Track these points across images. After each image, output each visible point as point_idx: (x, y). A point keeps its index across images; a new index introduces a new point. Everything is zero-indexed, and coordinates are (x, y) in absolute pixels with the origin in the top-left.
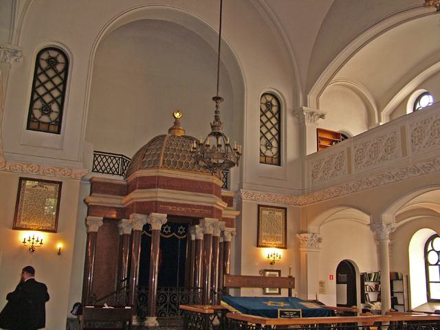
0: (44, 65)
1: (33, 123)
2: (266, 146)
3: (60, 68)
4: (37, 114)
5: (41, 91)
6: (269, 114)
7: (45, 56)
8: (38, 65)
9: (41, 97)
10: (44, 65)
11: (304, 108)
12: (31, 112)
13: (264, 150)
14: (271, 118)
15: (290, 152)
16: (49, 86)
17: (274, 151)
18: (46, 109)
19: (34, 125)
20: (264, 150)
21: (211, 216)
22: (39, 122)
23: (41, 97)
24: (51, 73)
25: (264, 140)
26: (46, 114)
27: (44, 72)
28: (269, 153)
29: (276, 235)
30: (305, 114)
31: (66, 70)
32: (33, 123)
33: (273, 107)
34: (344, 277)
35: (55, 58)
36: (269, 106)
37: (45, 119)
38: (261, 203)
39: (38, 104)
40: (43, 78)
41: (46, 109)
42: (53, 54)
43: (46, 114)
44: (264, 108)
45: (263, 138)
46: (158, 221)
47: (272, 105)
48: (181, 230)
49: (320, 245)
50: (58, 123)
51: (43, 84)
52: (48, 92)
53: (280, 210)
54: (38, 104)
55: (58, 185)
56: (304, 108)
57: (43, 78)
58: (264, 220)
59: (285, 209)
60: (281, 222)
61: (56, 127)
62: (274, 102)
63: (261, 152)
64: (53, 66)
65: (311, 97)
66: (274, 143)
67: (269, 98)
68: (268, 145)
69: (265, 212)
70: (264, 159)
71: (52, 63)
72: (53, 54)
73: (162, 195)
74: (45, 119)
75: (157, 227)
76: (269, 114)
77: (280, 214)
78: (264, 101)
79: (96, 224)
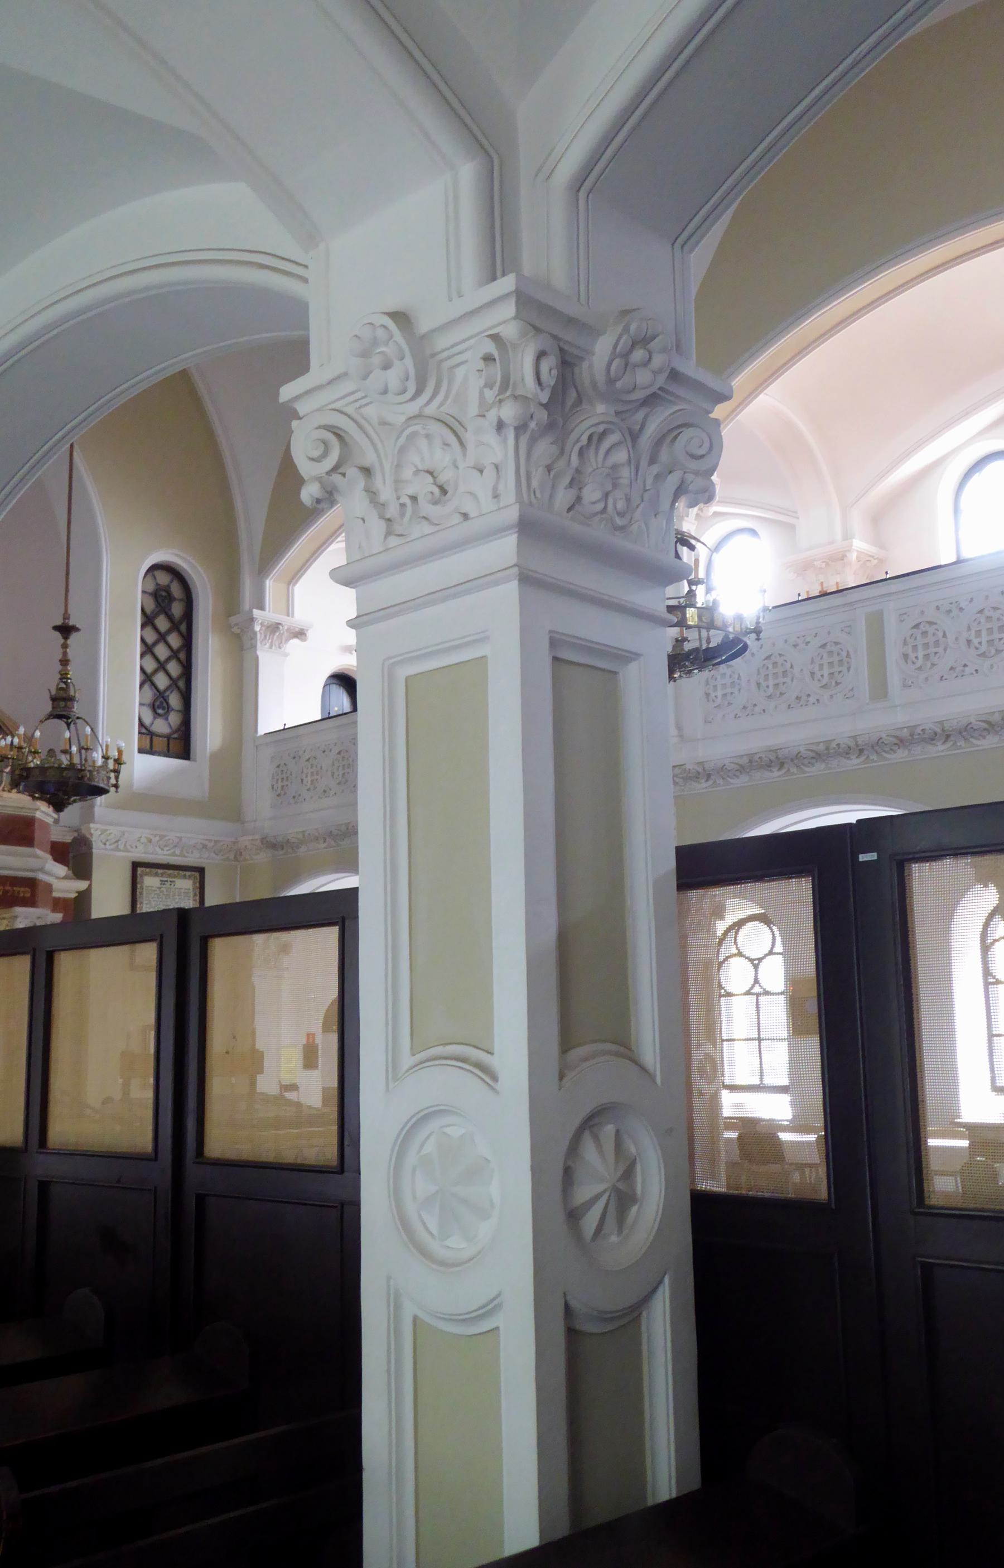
2: (154, 707)
11: (256, 612)
15: (210, 730)
17: (175, 719)
25: (149, 694)
28: (161, 727)
30: (257, 628)
33: (170, 608)
44: (151, 606)
45: (146, 687)
47: (171, 598)
53: (188, 873)
56: (256, 612)
59: (201, 871)
62: (176, 590)
63: (141, 724)
65: (270, 585)
66: (174, 700)
67: (163, 578)
68: (158, 705)
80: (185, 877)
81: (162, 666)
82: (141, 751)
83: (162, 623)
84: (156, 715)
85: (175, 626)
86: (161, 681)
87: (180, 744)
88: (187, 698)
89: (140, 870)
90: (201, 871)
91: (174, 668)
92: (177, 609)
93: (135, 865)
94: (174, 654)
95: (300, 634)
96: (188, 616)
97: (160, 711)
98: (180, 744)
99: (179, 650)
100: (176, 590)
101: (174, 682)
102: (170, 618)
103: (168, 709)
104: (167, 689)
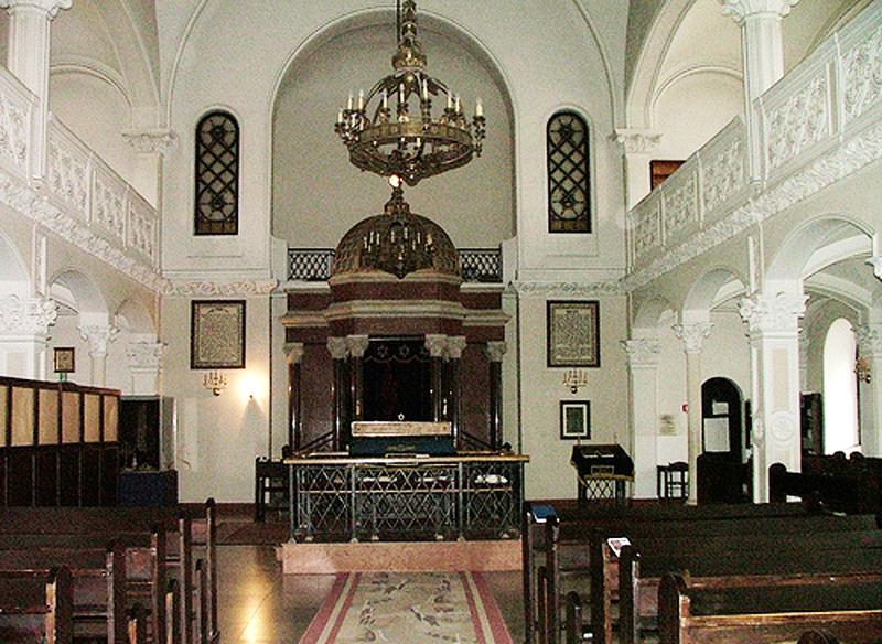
0: (208, 139)
1: (202, 226)
2: (562, 202)
3: (229, 139)
4: (206, 210)
5: (208, 177)
6: (566, 149)
7: (207, 127)
8: (199, 140)
9: (208, 187)
10: (208, 139)
13: (558, 208)
14: (571, 153)
16: (218, 168)
17: (579, 208)
18: (218, 202)
19: (205, 228)
20: (558, 208)
22: (211, 222)
24: (218, 150)
26: (215, 211)
27: (209, 150)
28: (569, 214)
29: (581, 346)
32: (202, 226)
34: (720, 407)
35: (221, 127)
36: (566, 133)
37: (218, 216)
39: (207, 197)
40: (208, 159)
43: (215, 211)
44: (556, 138)
47: (572, 132)
48: (405, 351)
50: (234, 218)
51: (209, 168)
54: (207, 197)
55: (241, 306)
61: (229, 226)
62: (576, 125)
64: (217, 139)
66: (578, 196)
68: (567, 200)
70: (557, 224)
71: (218, 133)
72: (218, 121)
74: (218, 216)
75: (358, 352)
76: (566, 149)
77: (585, 312)
78: (556, 126)
80: (584, 308)
81: (567, 176)
84: (565, 208)
85: (576, 149)
86: (568, 185)
89: (552, 305)
90: (596, 303)
92: (577, 138)
97: (568, 204)
98: (583, 224)
99: (581, 163)
100: (576, 125)
101: (577, 185)
102: (572, 144)
103: (573, 202)
104: (572, 190)
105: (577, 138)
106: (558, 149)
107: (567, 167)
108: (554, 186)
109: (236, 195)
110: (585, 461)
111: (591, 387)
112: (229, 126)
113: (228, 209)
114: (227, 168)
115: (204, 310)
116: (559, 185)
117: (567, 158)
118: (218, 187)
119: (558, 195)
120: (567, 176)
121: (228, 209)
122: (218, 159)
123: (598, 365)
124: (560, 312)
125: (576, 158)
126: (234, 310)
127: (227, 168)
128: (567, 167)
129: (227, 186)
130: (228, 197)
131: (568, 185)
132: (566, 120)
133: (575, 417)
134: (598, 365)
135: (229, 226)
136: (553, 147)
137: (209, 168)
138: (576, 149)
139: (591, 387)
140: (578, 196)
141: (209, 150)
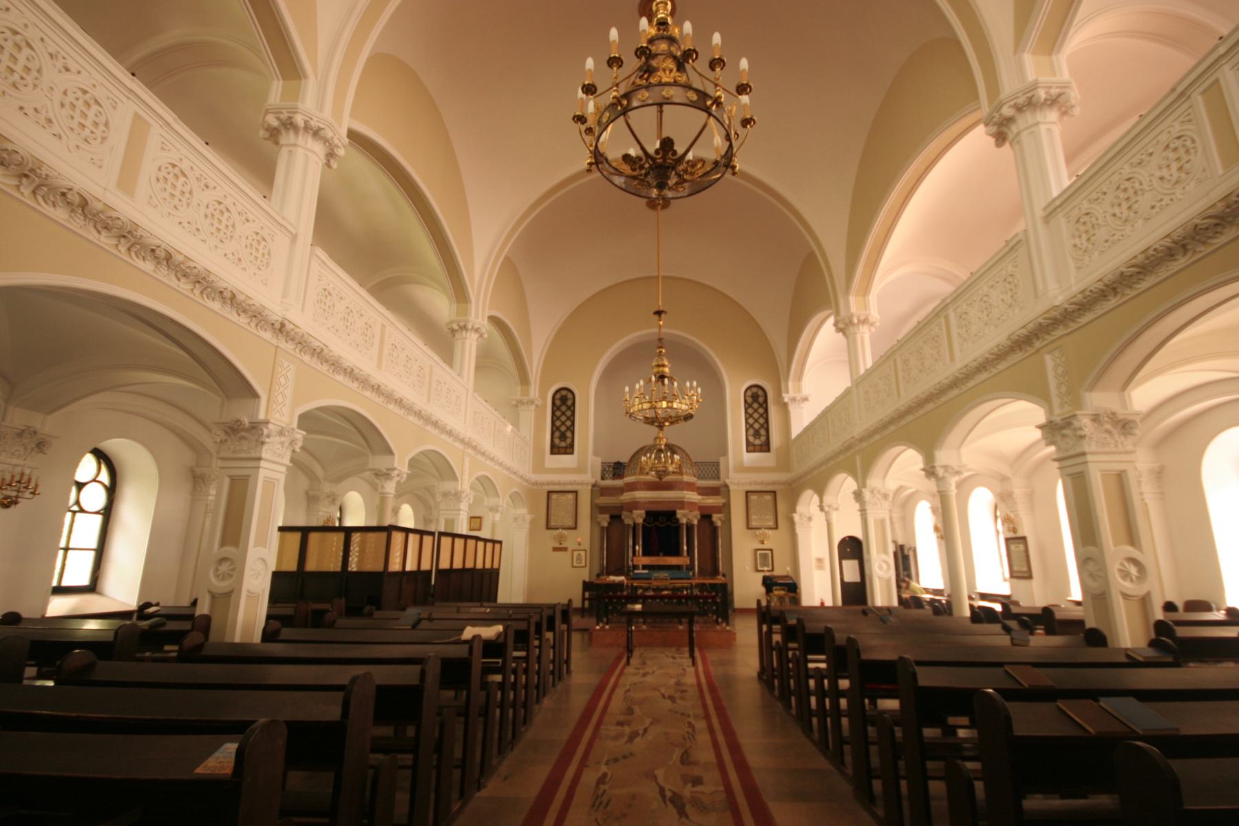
1: (555, 450)
3: (569, 403)
4: (557, 441)
5: (558, 423)
7: (558, 396)
9: (558, 428)
10: (558, 403)
12: (552, 441)
13: (751, 439)
15: (775, 440)
16: (563, 418)
17: (763, 439)
18: (563, 437)
20: (751, 439)
21: (682, 508)
23: (558, 428)
24: (564, 408)
26: (562, 442)
27: (559, 408)
28: (757, 442)
31: (574, 404)
32: (555, 450)
33: (757, 401)
36: (755, 397)
37: (563, 444)
38: (749, 488)
39: (557, 434)
40: (558, 413)
41: (563, 437)
42: (564, 393)
43: (562, 442)
44: (750, 400)
46: (639, 516)
49: (812, 523)
50: (572, 446)
51: (558, 418)
52: (563, 423)
57: (558, 413)
58: (751, 505)
59: (774, 492)
60: (771, 504)
62: (760, 393)
66: (763, 432)
67: (754, 390)
68: (757, 434)
69: (753, 497)
70: (751, 447)
71: (564, 400)
72: (564, 393)
73: (641, 495)
74: (563, 444)
75: (640, 521)
76: (755, 406)
77: (768, 497)
78: (749, 393)
79: (604, 520)
81: (756, 421)
82: (748, 451)
83: (755, 406)
85: (761, 405)
86: (757, 426)
87: (766, 447)
88: (767, 430)
91: (762, 421)
92: (761, 400)
93: (747, 492)
94: (761, 416)
95: (806, 399)
96: (766, 401)
98: (766, 447)
101: (762, 426)
105: (761, 400)
106: (750, 406)
107: (756, 416)
108: (749, 426)
109: (573, 433)
110: (769, 583)
111: (774, 540)
112: (570, 396)
113: (569, 441)
114: (568, 418)
115: (554, 496)
116: (751, 426)
117: (756, 411)
118: (563, 428)
119: (751, 431)
120: (756, 421)
121: (569, 441)
122: (563, 413)
123: (777, 528)
124: (753, 497)
125: (761, 411)
126: (570, 496)
127: (568, 418)
128: (756, 416)
129: (568, 428)
130: (569, 434)
131: (757, 426)
132: (754, 390)
133: (763, 557)
134: (777, 528)
135: (569, 450)
136: (748, 405)
137: (558, 418)
138: (761, 405)
139: (774, 540)
140: (763, 432)
141: (559, 408)
